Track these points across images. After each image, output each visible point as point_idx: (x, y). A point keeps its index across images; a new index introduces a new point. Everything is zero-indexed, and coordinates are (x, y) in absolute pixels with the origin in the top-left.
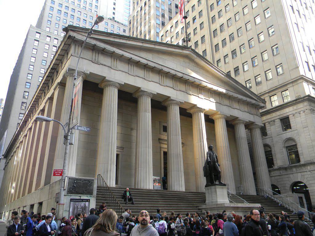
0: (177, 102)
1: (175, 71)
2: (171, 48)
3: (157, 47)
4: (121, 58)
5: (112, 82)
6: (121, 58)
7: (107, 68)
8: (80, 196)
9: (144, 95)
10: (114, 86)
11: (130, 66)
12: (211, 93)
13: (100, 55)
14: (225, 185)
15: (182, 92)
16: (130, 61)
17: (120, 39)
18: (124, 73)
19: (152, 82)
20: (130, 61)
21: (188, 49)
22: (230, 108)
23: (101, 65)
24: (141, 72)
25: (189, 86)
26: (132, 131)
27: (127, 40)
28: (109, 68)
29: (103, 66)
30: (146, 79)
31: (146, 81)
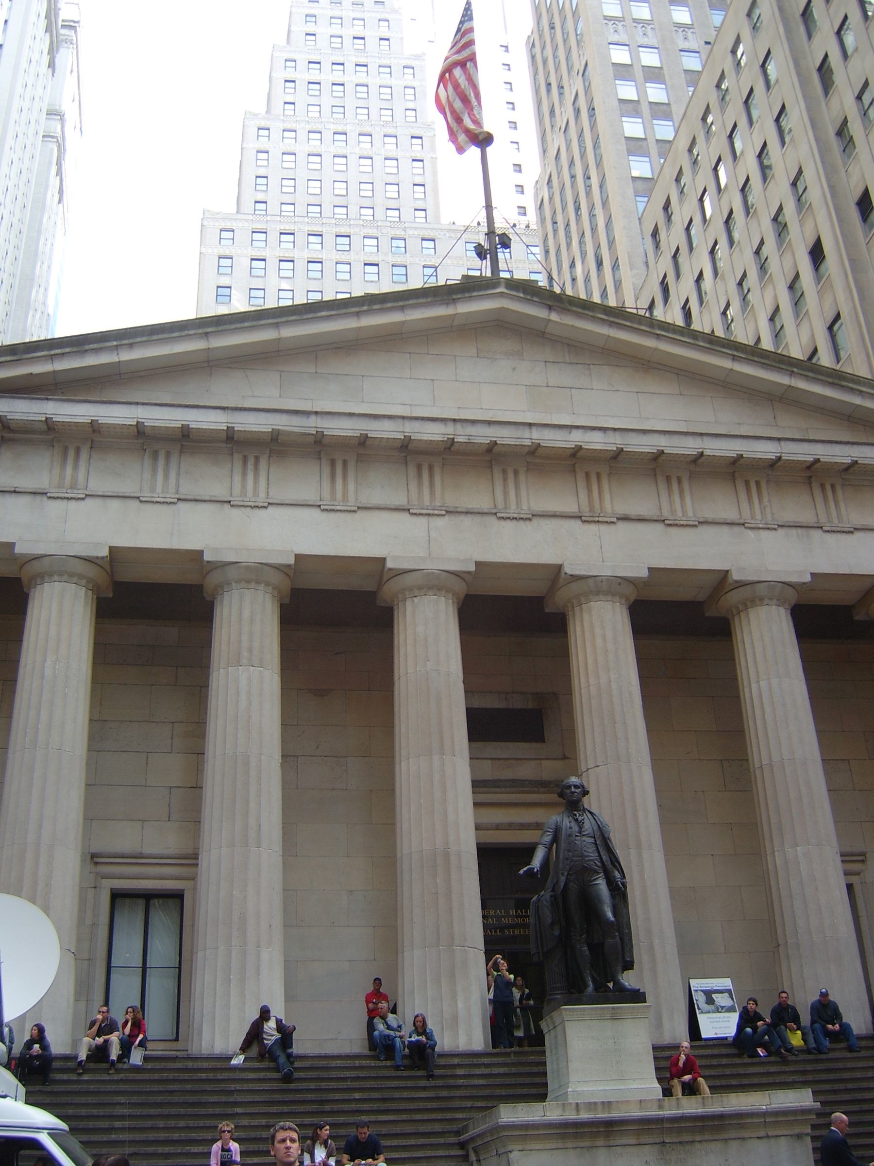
2: (382, 310)
3: (288, 332)
4: (94, 439)
5: (46, 560)
9: (229, 584)
10: (61, 574)
12: (668, 479)
14: (637, 996)
15: (467, 520)
18: (115, 504)
19: (271, 509)
20: (144, 441)
21: (487, 287)
22: (816, 534)
24: (211, 478)
25: (511, 475)
28: (38, 498)
29: (7, 495)
30: (236, 499)
31: (235, 512)
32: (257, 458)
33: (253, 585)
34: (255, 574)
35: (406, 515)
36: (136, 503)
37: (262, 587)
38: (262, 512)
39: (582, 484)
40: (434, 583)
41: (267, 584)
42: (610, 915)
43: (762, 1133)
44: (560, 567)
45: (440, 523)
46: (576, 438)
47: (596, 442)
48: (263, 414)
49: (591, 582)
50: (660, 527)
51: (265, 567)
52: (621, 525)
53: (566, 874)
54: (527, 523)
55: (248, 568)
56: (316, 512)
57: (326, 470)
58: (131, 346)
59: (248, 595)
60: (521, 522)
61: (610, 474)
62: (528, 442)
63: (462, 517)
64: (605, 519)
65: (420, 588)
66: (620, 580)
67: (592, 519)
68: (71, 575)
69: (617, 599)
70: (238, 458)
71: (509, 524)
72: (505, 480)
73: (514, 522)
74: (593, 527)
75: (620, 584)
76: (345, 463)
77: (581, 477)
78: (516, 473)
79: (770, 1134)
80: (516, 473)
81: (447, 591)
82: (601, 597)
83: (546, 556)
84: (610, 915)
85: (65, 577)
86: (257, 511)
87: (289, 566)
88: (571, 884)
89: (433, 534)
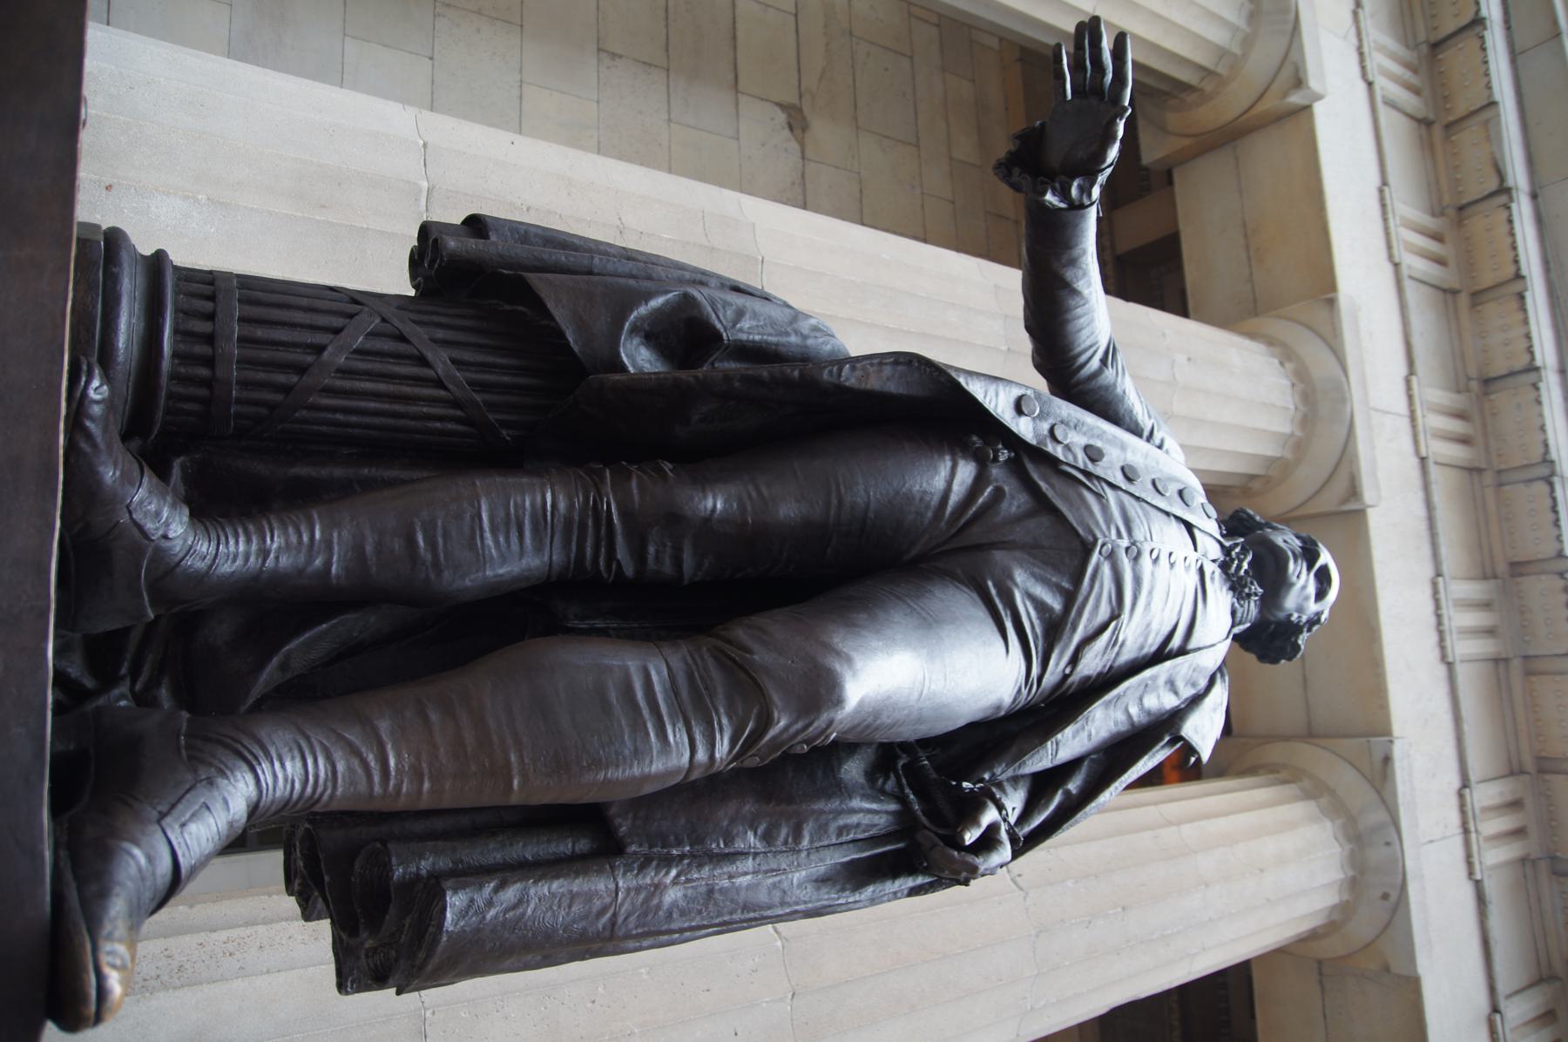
0: (1340, 394)
26: (781, 117)
35: (1402, 370)
37: (1241, 23)
38: (1355, 70)
41: (1248, 42)
49: (1380, 816)
51: (1290, 27)
52: (1467, 890)
53: (1025, 428)
60: (1434, 638)
63: (1420, 495)
66: (1394, 895)
67: (1470, 814)
73: (1433, 620)
74: (1454, 818)
75: (1385, 896)
78: (1490, 632)
80: (1490, 632)
86: (1355, 58)
88: (966, 472)
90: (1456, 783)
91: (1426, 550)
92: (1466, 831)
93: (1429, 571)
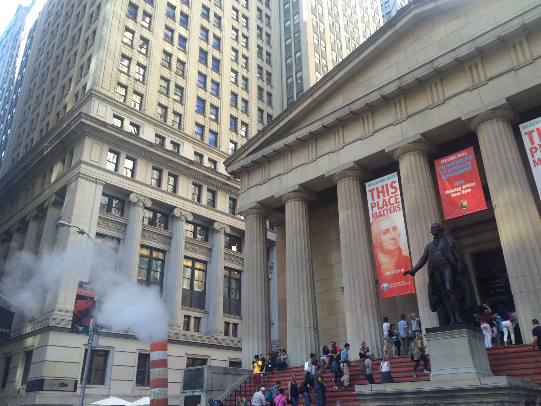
1: (378, 91)
3: (336, 78)
6: (290, 149)
7: (277, 178)
8: (193, 392)
11: (307, 149)
13: (267, 167)
15: (416, 117)
16: (303, 143)
17: (279, 122)
18: (299, 168)
19: (345, 148)
20: (303, 143)
23: (270, 181)
24: (326, 145)
27: (287, 115)
31: (334, 154)
32: (338, 131)
33: (344, 179)
34: (344, 174)
35: (392, 127)
36: (304, 166)
37: (347, 178)
38: (342, 150)
39: (468, 73)
40: (406, 150)
41: (349, 176)
42: (448, 287)
43: (479, 401)
44: (460, 118)
45: (406, 123)
46: (454, 55)
47: (464, 51)
48: (332, 115)
49: (477, 117)
50: (512, 74)
52: (490, 83)
54: (443, 105)
55: (339, 174)
56: (359, 142)
57: (361, 123)
58: (291, 112)
59: (343, 183)
60: (440, 106)
61: (482, 60)
62: (432, 70)
63: (415, 116)
64: (480, 85)
65: (402, 154)
68: (292, 198)
69: (500, 119)
70: (332, 133)
71: (435, 109)
72: (432, 90)
73: (437, 107)
74: (476, 91)
75: (492, 113)
76: (367, 117)
77: (467, 68)
79: (484, 401)
81: (415, 151)
82: (486, 123)
83: (454, 117)
84: (448, 287)
85: (291, 200)
86: (340, 151)
87: (352, 167)
89: (403, 130)
90: (468, 92)
91: (424, 112)
92: (478, 87)
93: (428, 110)
